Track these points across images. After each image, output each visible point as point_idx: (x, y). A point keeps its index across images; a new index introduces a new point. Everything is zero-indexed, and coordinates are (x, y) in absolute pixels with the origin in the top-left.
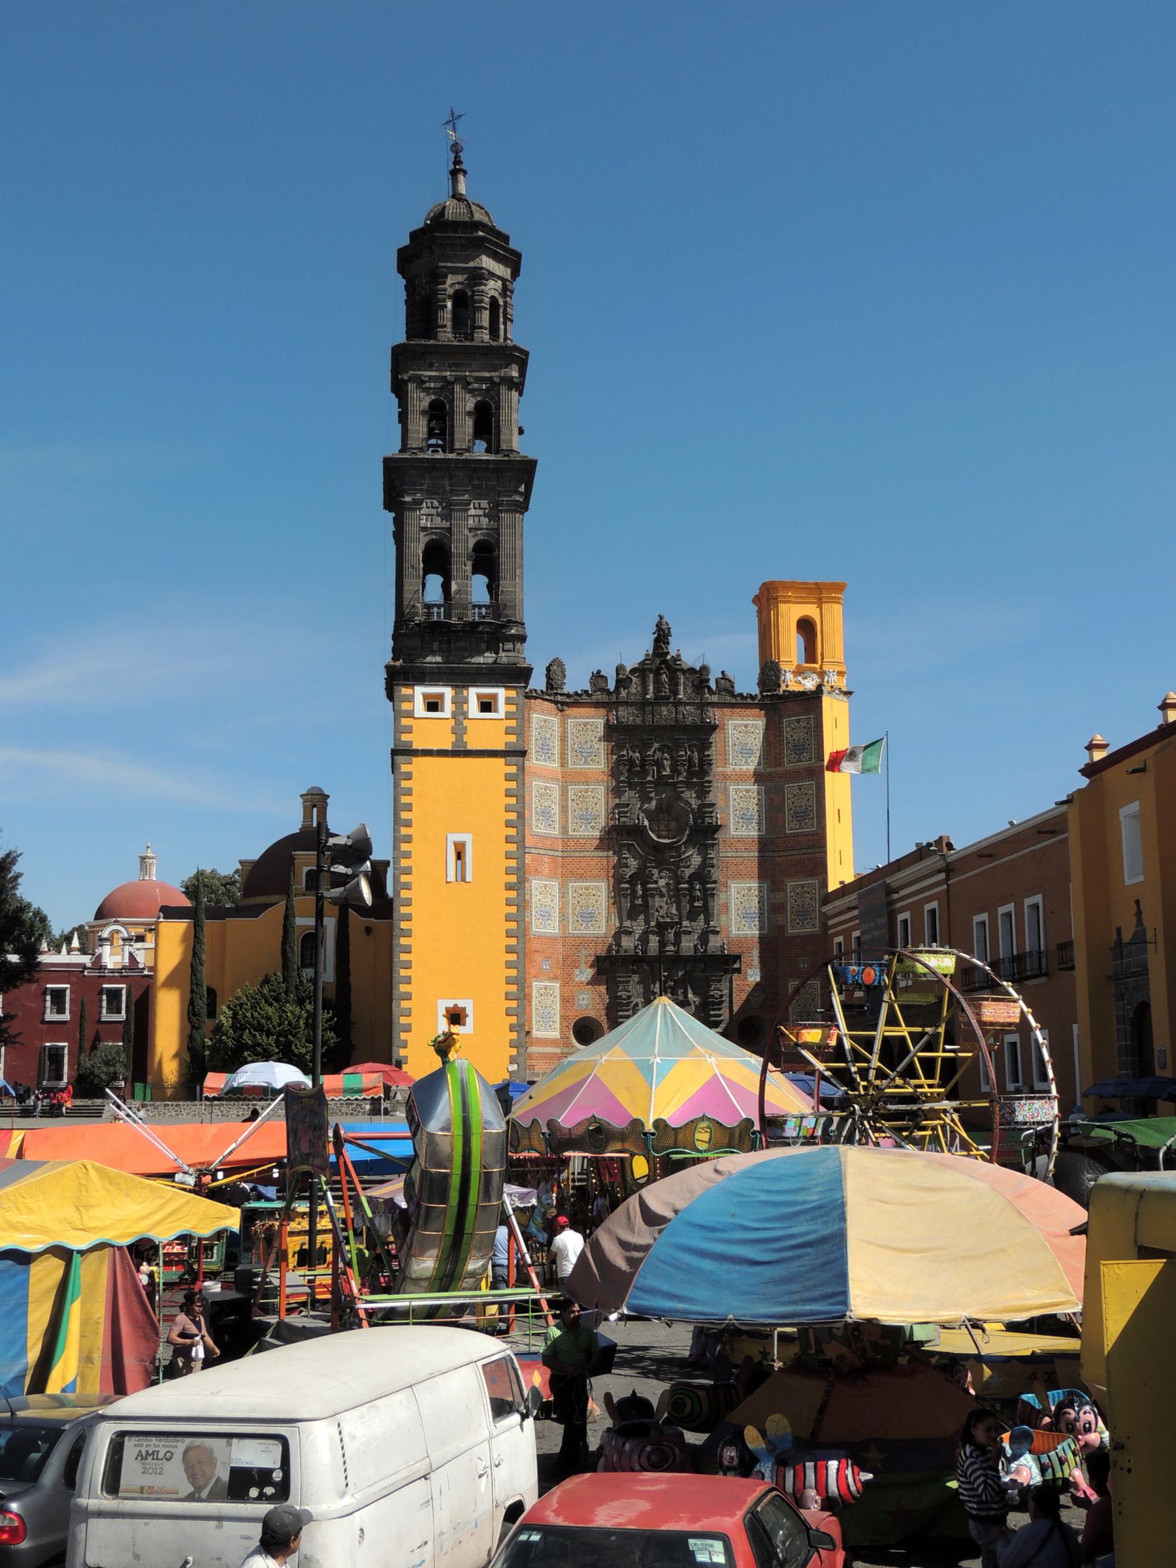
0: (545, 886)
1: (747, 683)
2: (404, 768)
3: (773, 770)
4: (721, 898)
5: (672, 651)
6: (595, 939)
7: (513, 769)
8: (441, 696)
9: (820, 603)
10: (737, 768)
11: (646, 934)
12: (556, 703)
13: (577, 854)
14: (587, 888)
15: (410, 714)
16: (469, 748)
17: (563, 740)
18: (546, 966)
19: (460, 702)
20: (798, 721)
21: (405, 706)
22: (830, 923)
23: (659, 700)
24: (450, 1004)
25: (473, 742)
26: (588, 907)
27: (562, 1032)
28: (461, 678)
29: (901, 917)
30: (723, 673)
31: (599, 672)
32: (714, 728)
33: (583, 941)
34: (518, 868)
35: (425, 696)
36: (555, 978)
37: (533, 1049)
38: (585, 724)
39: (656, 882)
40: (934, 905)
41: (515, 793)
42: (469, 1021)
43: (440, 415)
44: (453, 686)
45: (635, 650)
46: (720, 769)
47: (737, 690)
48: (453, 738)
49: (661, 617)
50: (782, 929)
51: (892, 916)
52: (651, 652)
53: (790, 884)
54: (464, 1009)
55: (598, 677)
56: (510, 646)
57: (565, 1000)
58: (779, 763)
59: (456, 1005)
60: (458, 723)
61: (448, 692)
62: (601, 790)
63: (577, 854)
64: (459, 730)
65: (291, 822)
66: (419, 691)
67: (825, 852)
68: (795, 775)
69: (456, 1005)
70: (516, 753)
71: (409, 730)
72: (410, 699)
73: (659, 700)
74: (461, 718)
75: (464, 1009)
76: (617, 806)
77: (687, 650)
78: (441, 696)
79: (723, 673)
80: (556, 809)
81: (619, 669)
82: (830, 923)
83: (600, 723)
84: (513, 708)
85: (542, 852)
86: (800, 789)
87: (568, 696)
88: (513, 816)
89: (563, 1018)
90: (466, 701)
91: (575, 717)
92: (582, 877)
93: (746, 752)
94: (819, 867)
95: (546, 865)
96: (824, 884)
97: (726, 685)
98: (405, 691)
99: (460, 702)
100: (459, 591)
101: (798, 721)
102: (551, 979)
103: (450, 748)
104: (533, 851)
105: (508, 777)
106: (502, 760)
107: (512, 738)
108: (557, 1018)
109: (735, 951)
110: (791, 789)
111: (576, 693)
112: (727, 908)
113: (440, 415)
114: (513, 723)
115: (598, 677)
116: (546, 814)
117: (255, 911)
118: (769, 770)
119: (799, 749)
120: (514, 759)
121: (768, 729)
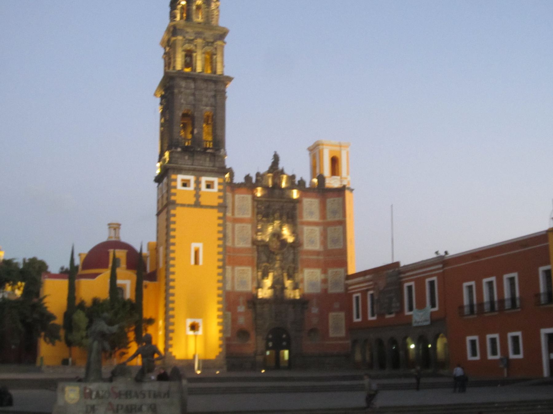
7: (221, 215)
8: (189, 181)
14: (243, 270)
15: (175, 187)
19: (198, 183)
20: (334, 201)
22: (350, 288)
25: (204, 201)
29: (406, 285)
33: (241, 294)
35: (183, 180)
38: (243, 197)
43: (189, 55)
45: (264, 167)
49: (275, 152)
50: (326, 290)
51: (401, 285)
56: (220, 159)
57: (234, 321)
61: (192, 178)
62: (249, 226)
64: (197, 195)
65: (102, 236)
66: (180, 178)
70: (222, 207)
71: (175, 194)
72: (175, 180)
78: (189, 181)
81: (258, 175)
83: (249, 197)
84: (221, 187)
87: (235, 184)
92: (241, 264)
93: (311, 213)
94: (343, 263)
96: (346, 271)
97: (302, 183)
98: (173, 177)
99: (198, 183)
100: (198, 133)
101: (334, 201)
105: (219, 218)
107: (221, 201)
110: (330, 229)
112: (302, 281)
113: (189, 55)
117: (94, 276)
119: (334, 212)
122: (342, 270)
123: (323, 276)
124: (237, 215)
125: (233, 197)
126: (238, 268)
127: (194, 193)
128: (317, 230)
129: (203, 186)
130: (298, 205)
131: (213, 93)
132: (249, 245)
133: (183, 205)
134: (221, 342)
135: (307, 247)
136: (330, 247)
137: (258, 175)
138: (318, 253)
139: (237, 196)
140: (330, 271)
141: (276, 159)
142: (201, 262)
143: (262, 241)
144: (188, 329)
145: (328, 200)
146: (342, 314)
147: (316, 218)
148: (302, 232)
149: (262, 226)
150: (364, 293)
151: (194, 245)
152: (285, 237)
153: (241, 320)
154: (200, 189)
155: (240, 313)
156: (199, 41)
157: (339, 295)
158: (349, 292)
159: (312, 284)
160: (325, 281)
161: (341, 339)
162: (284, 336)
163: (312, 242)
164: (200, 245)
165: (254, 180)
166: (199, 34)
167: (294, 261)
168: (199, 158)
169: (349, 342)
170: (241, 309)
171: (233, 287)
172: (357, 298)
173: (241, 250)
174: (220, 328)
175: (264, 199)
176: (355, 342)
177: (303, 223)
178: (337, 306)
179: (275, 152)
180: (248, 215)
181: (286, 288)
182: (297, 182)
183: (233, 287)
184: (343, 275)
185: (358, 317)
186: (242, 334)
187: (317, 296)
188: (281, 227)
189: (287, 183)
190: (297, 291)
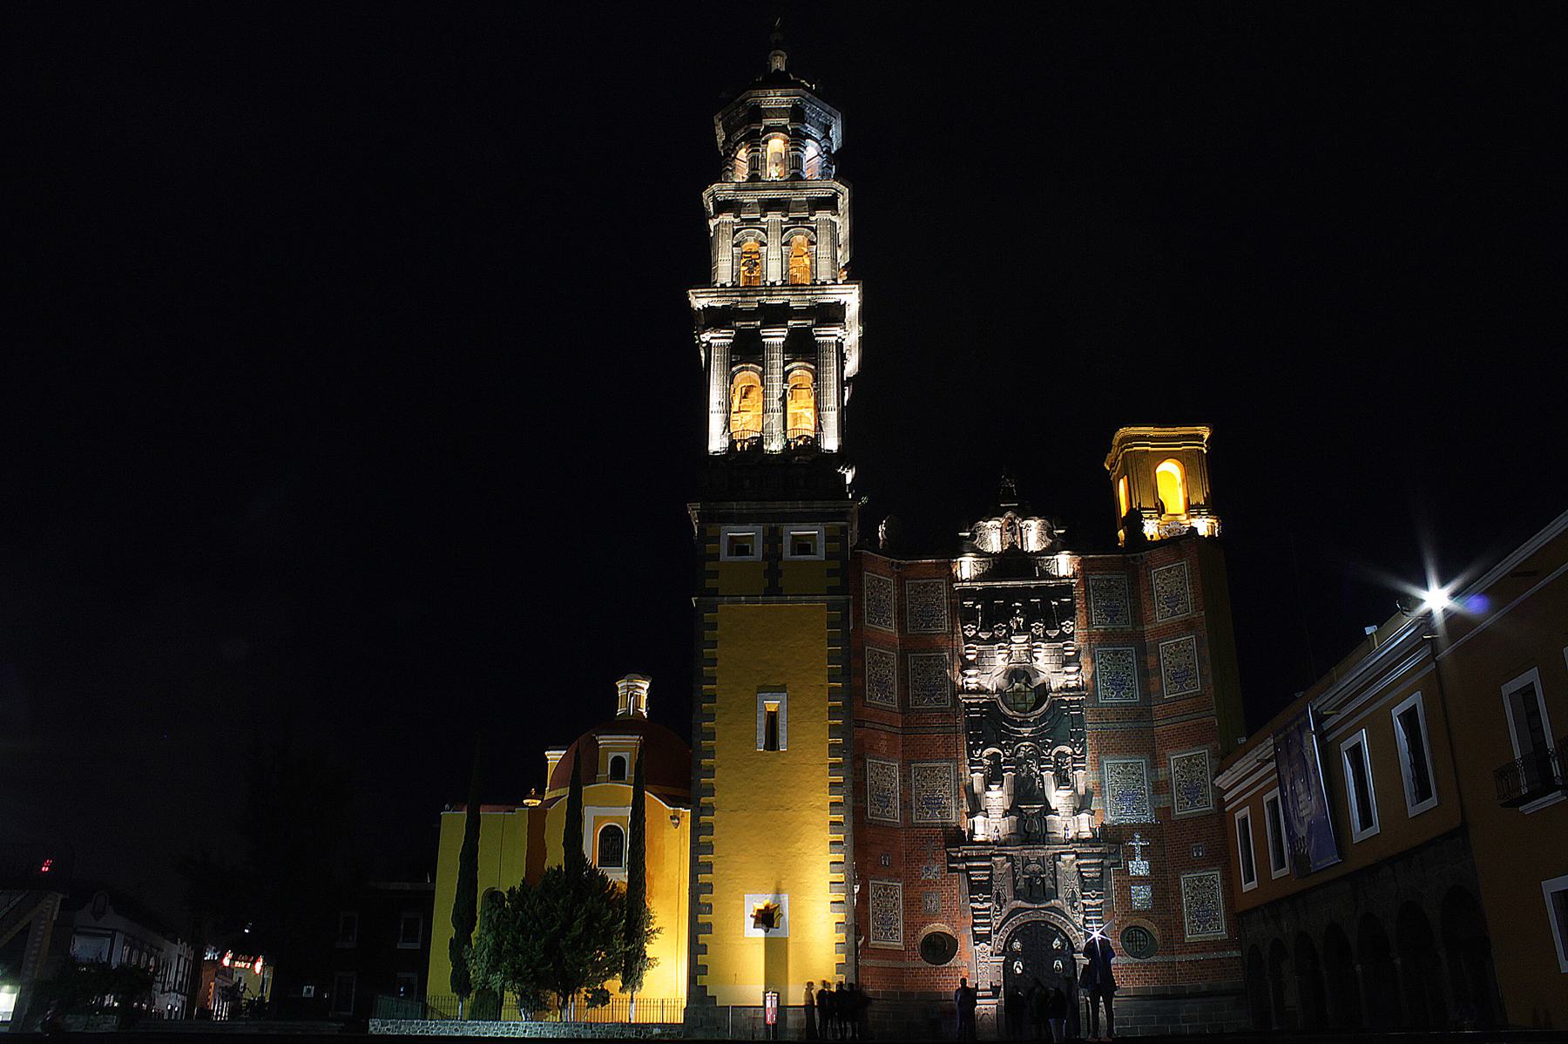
15: (716, 557)
20: (1169, 570)
22: (1227, 798)
40: (1415, 699)
50: (1168, 811)
72: (717, 539)
80: (894, 679)
82: (1227, 798)
114: (836, 564)
134: (842, 958)
143: (980, 691)
146: (1217, 874)
149: (980, 654)
150: (1255, 802)
152: (1042, 678)
156: (774, 217)
161: (1217, 945)
166: (768, 206)
174: (841, 917)
175: (979, 585)
181: (1055, 812)
188: (1030, 653)
189: (1040, 540)
190: (1084, 816)
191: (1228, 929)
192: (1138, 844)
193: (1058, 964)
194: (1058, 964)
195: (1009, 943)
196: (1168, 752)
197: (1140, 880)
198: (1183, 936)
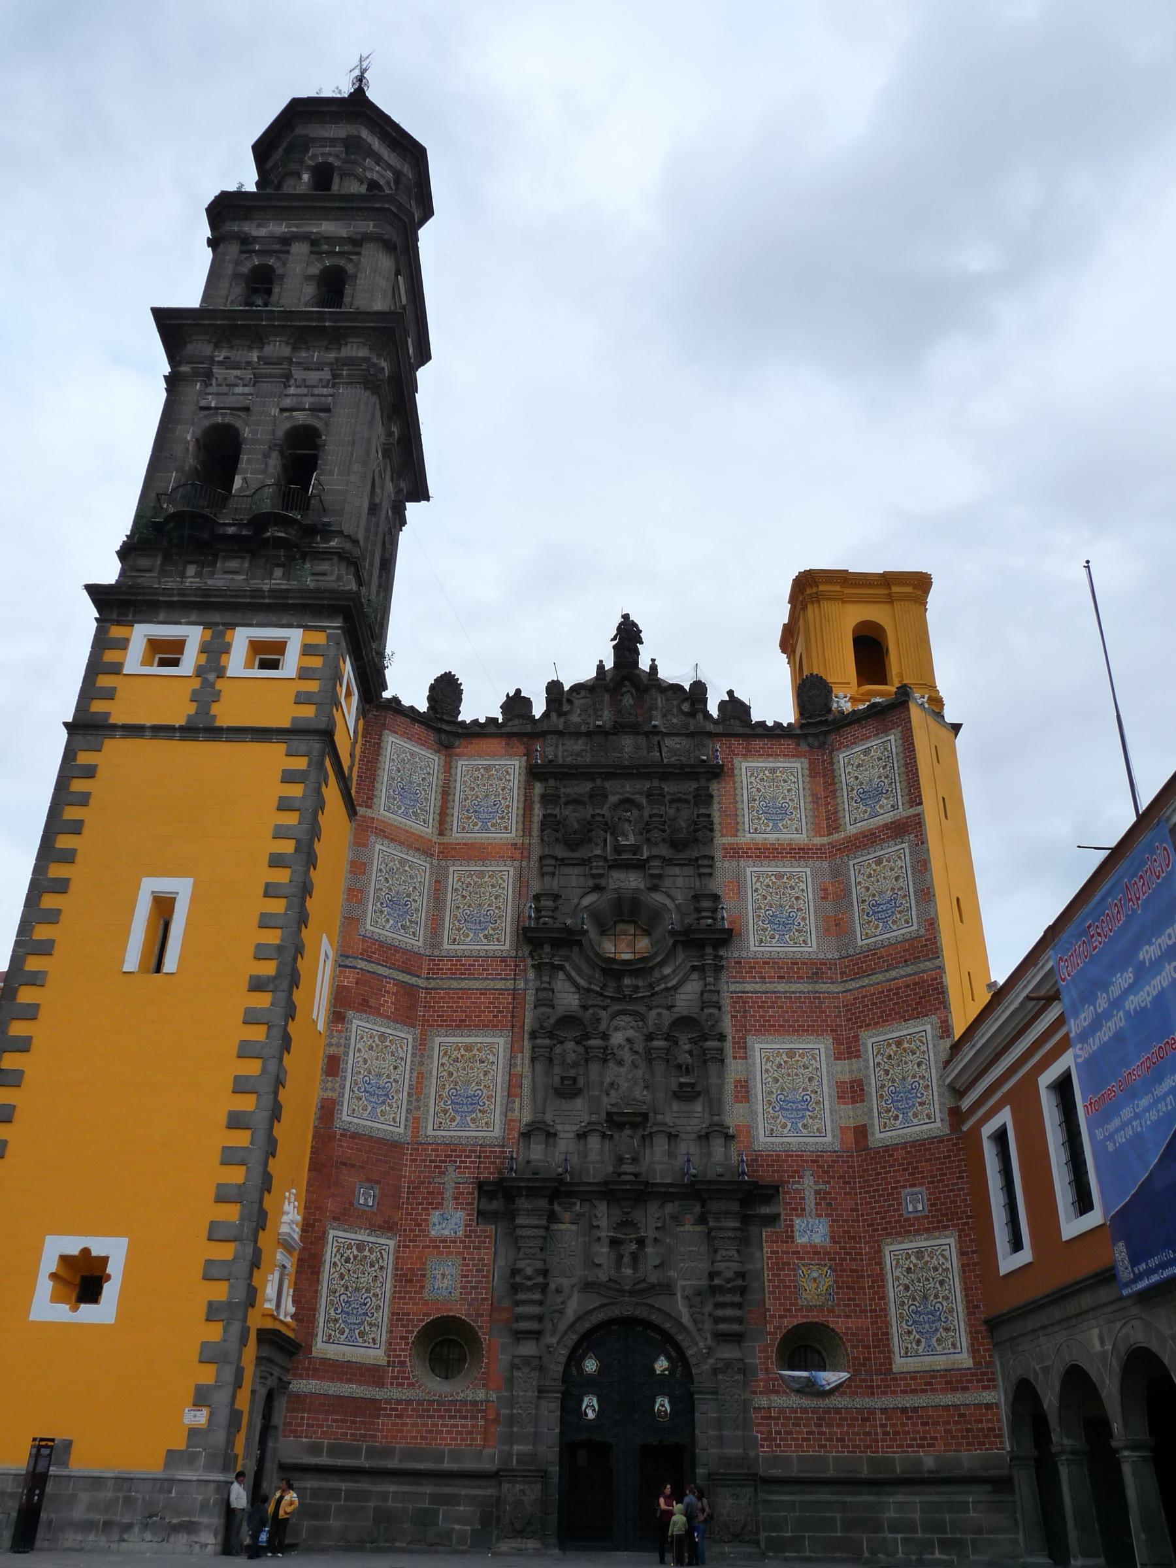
0: (383, 1037)
1: (773, 701)
2: (84, 758)
3: (825, 840)
4: (734, 1069)
5: (644, 664)
6: (480, 1150)
7: (301, 763)
9: (890, 600)
10: (759, 838)
11: (582, 1136)
12: (439, 731)
13: (455, 984)
14: (469, 1048)
15: (116, 669)
16: (219, 723)
17: (446, 793)
18: (366, 1198)
19: (215, 651)
20: (866, 752)
21: (110, 656)
22: (966, 1104)
23: (619, 728)
24: (72, 1246)
25: (226, 714)
26: (469, 1083)
27: (390, 1350)
28: (220, 610)
30: (730, 693)
31: (518, 691)
32: (717, 772)
33: (452, 1152)
34: (280, 949)
36: (388, 1228)
37: (302, 1385)
38: (488, 769)
39: (605, 1037)
41: (297, 805)
42: (110, 1291)
44: (207, 625)
46: (727, 840)
47: (756, 717)
48: (192, 709)
49: (626, 617)
50: (861, 1132)
52: (609, 664)
53: (870, 1040)
54: (104, 1260)
55: (516, 704)
57: (408, 1278)
58: (833, 825)
59: (86, 1251)
60: (206, 684)
61: (193, 635)
63: (455, 984)
66: (141, 634)
67: (941, 969)
68: (868, 840)
69: (86, 1251)
72: (123, 644)
73: (619, 728)
74: (211, 677)
75: (104, 1260)
76: (537, 898)
77: (668, 658)
79: (730, 693)
80: (422, 903)
81: (554, 688)
82: (966, 1104)
85: (381, 970)
86: (879, 862)
88: (287, 847)
89: (397, 1318)
90: (226, 649)
91: (470, 757)
92: (460, 1025)
94: (929, 996)
95: (389, 999)
97: (735, 708)
99: (215, 651)
101: (866, 752)
102: (373, 1228)
103: (180, 721)
104: (362, 964)
105: (289, 777)
106: (281, 748)
107: (308, 711)
108: (383, 1317)
109: (767, 1176)
111: (476, 722)
112: (744, 1091)
114: (313, 686)
115: (516, 704)
116: (398, 905)
118: (818, 841)
119: (870, 796)
120: (301, 744)
121: (813, 774)
122: (926, 1027)
123: (845, 1070)
124: (456, 835)
125: (448, 769)
126: (441, 1040)
127: (196, 684)
128: (805, 878)
129: (237, 662)
130: (715, 788)
131: (326, 374)
132: (504, 943)
133: (135, 731)
135: (757, 942)
136: (867, 935)
137: (554, 688)
138: (816, 970)
139: (462, 766)
140: (870, 1040)
141: (628, 636)
142: (171, 964)
144: (45, 1287)
145: (841, 757)
146: (948, 1243)
147: (797, 830)
148: (738, 884)
151: (150, 886)
153: (447, 1285)
154: (221, 672)
155: (441, 1245)
157: (918, 1148)
158: (965, 1128)
159: (796, 1108)
160: (853, 1092)
161: (952, 1380)
162: (661, 1365)
163: (784, 925)
164: (181, 887)
165: (539, 709)
167: (710, 1001)
168: (233, 564)
169: (997, 1396)
170: (449, 1222)
171: (416, 1124)
172: (1000, 1137)
173: (462, 966)
176: (1024, 1394)
177: (736, 853)
178: (915, 1202)
179: (626, 617)
180: (508, 832)
182: (713, 709)
183: (416, 1124)
184: (934, 1052)
185: (1017, 1245)
186: (446, 1344)
187: (821, 1163)
191: (974, 1351)
192: (808, 1185)
193: (663, 1404)
194: (663, 1404)
195: (575, 1358)
196: (864, 1034)
197: (816, 1252)
198: (889, 1359)
